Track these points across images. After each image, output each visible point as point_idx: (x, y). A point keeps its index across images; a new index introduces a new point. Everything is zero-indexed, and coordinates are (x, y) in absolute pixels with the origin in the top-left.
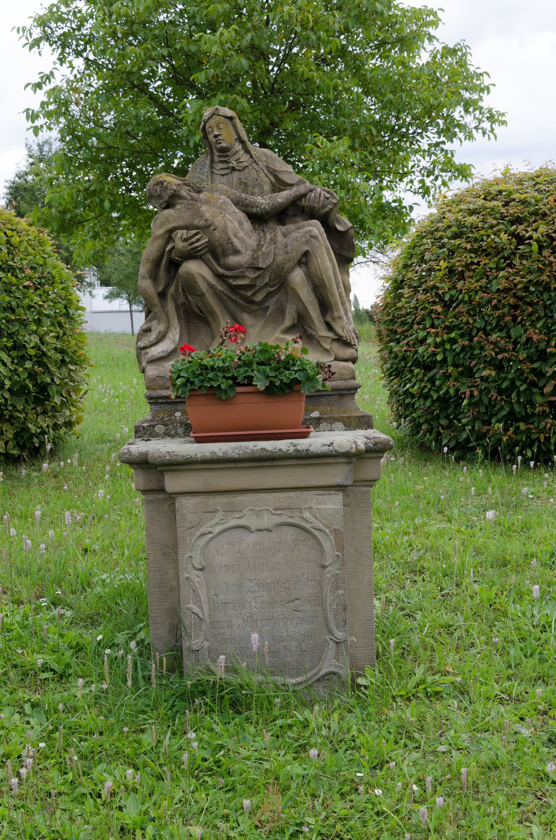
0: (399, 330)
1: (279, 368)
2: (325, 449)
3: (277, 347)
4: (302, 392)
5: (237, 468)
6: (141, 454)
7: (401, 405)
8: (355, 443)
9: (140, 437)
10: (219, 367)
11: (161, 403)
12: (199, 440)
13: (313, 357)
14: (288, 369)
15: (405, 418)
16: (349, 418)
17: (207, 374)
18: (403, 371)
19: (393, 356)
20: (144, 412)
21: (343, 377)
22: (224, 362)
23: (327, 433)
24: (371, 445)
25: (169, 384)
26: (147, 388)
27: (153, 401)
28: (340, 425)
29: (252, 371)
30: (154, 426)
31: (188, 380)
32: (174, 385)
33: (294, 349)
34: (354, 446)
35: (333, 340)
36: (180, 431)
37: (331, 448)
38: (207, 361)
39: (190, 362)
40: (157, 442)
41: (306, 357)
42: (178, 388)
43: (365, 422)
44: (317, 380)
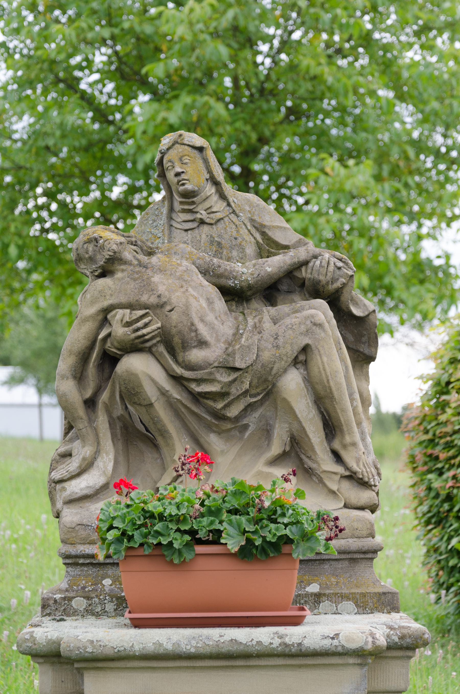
0: (443, 456)
1: (261, 520)
2: (327, 644)
3: (259, 488)
4: (295, 556)
5: (194, 668)
6: (50, 642)
7: (442, 569)
8: (372, 635)
9: (49, 614)
10: (171, 515)
11: (83, 564)
12: (138, 624)
13: (312, 503)
14: (275, 521)
15: (448, 589)
16: (363, 595)
17: (153, 525)
18: (447, 517)
19: (432, 494)
20: (56, 577)
21: (357, 533)
22: (178, 508)
23: (330, 617)
24: (396, 639)
25: (95, 536)
26: (63, 541)
27: (71, 561)
28: (350, 605)
29: (221, 522)
30: (70, 599)
31: (124, 533)
32: (104, 540)
33: (284, 490)
34: (370, 639)
35: (344, 477)
36: (110, 607)
37: (335, 642)
38: (154, 506)
39: (128, 506)
40: (75, 624)
41: (301, 503)
42: (109, 545)
43: (387, 602)
44: (317, 539)
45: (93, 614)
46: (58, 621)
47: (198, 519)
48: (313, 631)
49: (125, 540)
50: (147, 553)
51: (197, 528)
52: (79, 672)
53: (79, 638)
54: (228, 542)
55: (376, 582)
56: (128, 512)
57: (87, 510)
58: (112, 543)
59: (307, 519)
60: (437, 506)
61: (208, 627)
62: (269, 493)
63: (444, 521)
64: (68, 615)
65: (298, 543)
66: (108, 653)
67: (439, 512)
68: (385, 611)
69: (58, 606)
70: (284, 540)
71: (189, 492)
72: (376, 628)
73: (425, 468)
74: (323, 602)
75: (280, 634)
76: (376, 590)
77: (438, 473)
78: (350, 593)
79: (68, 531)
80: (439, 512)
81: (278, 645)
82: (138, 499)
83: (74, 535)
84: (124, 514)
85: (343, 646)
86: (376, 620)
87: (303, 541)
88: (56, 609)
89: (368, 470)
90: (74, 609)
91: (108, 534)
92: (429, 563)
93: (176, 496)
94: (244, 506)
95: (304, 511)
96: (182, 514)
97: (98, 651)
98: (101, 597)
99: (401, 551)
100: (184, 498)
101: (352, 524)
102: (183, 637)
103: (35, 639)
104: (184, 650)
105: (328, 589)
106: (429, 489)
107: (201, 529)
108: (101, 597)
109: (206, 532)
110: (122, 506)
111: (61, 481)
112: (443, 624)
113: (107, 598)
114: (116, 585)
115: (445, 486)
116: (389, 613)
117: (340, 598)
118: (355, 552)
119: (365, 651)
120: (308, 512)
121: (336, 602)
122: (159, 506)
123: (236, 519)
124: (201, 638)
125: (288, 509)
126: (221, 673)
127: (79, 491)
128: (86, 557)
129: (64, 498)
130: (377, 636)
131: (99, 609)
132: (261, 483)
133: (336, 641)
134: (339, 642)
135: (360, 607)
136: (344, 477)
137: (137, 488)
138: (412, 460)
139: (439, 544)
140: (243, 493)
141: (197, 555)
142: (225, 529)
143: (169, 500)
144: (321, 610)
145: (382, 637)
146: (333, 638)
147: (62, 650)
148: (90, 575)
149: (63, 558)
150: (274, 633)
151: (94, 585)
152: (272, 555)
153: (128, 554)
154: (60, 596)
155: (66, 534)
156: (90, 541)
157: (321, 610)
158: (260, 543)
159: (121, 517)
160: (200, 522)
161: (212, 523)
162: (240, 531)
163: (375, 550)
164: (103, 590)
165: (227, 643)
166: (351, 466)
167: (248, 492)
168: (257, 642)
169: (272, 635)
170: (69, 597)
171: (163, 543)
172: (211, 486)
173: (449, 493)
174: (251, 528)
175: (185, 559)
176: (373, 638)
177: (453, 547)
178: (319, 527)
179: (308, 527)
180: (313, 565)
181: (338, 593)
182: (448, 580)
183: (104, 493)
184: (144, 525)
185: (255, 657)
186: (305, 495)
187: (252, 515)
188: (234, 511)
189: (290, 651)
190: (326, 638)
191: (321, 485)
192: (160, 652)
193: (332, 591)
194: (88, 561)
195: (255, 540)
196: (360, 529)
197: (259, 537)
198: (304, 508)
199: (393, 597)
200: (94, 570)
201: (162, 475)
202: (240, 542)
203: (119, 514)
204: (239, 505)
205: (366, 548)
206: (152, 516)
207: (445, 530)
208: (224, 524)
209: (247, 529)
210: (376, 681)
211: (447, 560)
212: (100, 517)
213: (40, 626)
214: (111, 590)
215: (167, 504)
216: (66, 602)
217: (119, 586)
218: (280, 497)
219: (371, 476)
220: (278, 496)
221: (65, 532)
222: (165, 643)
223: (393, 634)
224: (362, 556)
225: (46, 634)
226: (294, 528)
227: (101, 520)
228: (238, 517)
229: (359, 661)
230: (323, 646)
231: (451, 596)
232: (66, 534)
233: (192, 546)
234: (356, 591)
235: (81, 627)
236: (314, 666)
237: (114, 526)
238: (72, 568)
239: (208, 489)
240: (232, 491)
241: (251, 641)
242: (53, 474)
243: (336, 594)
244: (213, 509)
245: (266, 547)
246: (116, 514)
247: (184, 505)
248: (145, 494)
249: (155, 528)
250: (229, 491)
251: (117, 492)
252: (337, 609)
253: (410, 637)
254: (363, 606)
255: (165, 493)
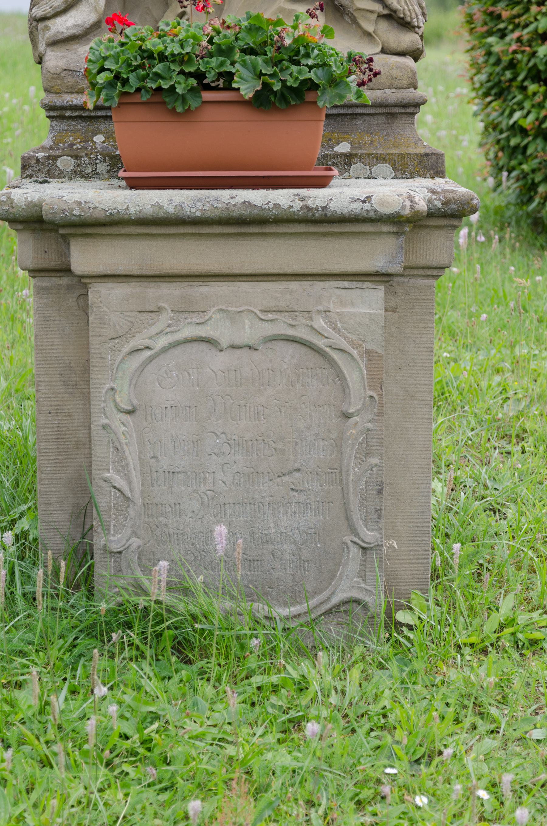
0: (505, 14)
1: (281, 61)
2: (357, 207)
3: (278, 23)
4: (320, 104)
5: (200, 235)
6: (31, 205)
7: (502, 149)
8: (411, 198)
9: (31, 176)
10: (173, 55)
11: (70, 118)
12: (134, 184)
13: (341, 44)
14: (297, 63)
15: (510, 172)
16: (403, 156)
17: (152, 66)
18: (509, 87)
19: (492, 60)
20: (39, 133)
21: (396, 83)
22: (182, 46)
23: (362, 181)
24: (439, 205)
25: (85, 84)
26: (46, 90)
27: (56, 113)
28: (386, 168)
29: (233, 64)
30: (55, 158)
31: (117, 77)
32: (93, 85)
33: (308, 26)
34: (408, 203)
35: (381, 16)
36: (102, 168)
37: (367, 206)
38: (153, 44)
39: (122, 44)
40: (60, 185)
41: (329, 43)
42: (100, 90)
43: (431, 165)
44: (347, 84)
45: (82, 177)
46: (41, 183)
47: (206, 59)
48: (341, 193)
49: (119, 84)
50: (144, 99)
51: (204, 70)
52: (65, 241)
53: (64, 198)
54: (242, 87)
55: (418, 141)
56: (123, 51)
57: (75, 53)
58: (104, 87)
59: (335, 61)
60: (498, 74)
61: (217, 189)
62: (291, 30)
63: (506, 93)
64: (53, 177)
65: (324, 89)
66: (98, 216)
67: (500, 81)
68: (428, 175)
69: (40, 166)
70: (309, 85)
71: (196, 27)
72: (415, 191)
73: (485, 28)
74: (355, 164)
75: (302, 196)
76: (418, 151)
77: (499, 34)
78: (386, 154)
79: (53, 78)
80: (500, 81)
81: (299, 209)
82: (135, 36)
83: (59, 82)
84: (118, 53)
85: (376, 211)
86: (418, 184)
87: (330, 87)
88: (39, 170)
89: (411, 8)
90: (60, 170)
91: (98, 77)
92: (486, 144)
93: (180, 32)
94: (260, 45)
95: (332, 52)
96: (187, 53)
97: (87, 214)
98: (92, 156)
99: (454, 132)
100: (189, 34)
101: (391, 71)
102: (187, 198)
103: (12, 202)
104: (189, 213)
105: (361, 149)
106: (489, 54)
107: (209, 71)
108: (92, 156)
109: (215, 75)
110: (116, 44)
111: (44, 19)
112: (502, 216)
113: (99, 157)
114: (110, 142)
115: (508, 50)
116: (433, 178)
117: (375, 160)
118: (394, 106)
119: (402, 216)
120: (337, 54)
121: (369, 164)
122: (159, 44)
123: (250, 59)
124: (208, 200)
125: (313, 49)
126: (232, 241)
127: (65, 31)
128: (74, 109)
129: (48, 38)
130: (417, 199)
131: (89, 170)
132: (281, 17)
133: (367, 204)
134: (372, 206)
135: (399, 170)
136: (381, 16)
137: (133, 24)
138: (469, 19)
139: (500, 119)
140: (259, 29)
141: (204, 102)
142: (238, 71)
143: (171, 37)
144: (351, 174)
145: (422, 201)
146: (364, 202)
147: (44, 213)
148: (78, 130)
149: (47, 110)
150: (294, 195)
151: (83, 142)
152: (293, 103)
153: (122, 101)
154: (43, 154)
155: (49, 81)
156: (79, 89)
157: (351, 174)
158: (279, 88)
159: (113, 56)
160: (208, 63)
161: (222, 64)
162: (255, 74)
163: (417, 103)
164: (94, 148)
165: (239, 205)
166: (390, 3)
167: (265, 27)
168: (274, 204)
169: (292, 197)
170: (54, 156)
171: (163, 87)
172: (221, 21)
173: (513, 59)
174: (269, 71)
175: (190, 106)
176: (412, 202)
177: (515, 123)
178: (350, 70)
179: (337, 70)
180: (343, 120)
181: (372, 154)
182: (509, 163)
183: (95, 33)
184: (142, 66)
185: (272, 222)
186: (334, 33)
187: (270, 55)
188: (249, 51)
189: (314, 216)
190: (355, 201)
191: (354, 26)
192: (160, 216)
193: (365, 152)
194: (76, 114)
195: (274, 84)
196: (399, 78)
197: (278, 82)
198: (332, 49)
199: (437, 159)
200: (83, 124)
201: (164, 12)
202: (255, 87)
203: (112, 53)
204: (254, 43)
205: (407, 101)
206: (151, 56)
207: (506, 103)
208: (237, 65)
209: (263, 72)
210: (415, 254)
211: (508, 139)
212: (89, 57)
213: (19, 187)
214: (104, 148)
215: (168, 41)
216: (51, 161)
217: (113, 144)
218: (304, 34)
219: (414, 16)
220: (301, 33)
221: (49, 79)
222: (165, 205)
223: (435, 199)
224: (402, 110)
225: (25, 195)
226: (320, 72)
227: (90, 61)
228: (253, 57)
229: (395, 229)
230: (352, 211)
231: (512, 181)
232: (49, 81)
233: (199, 92)
234: (395, 151)
235: (66, 189)
236: (342, 234)
237: (106, 67)
238: (57, 121)
239: (217, 24)
240: (246, 27)
241: (268, 204)
242: (34, 10)
243: (371, 154)
244: (224, 47)
245: (286, 93)
246: (108, 54)
247: (189, 42)
248: (143, 31)
249: (154, 70)
250: (243, 27)
251: (110, 29)
252: (371, 173)
253: (455, 202)
254: (401, 170)
255: (167, 29)
